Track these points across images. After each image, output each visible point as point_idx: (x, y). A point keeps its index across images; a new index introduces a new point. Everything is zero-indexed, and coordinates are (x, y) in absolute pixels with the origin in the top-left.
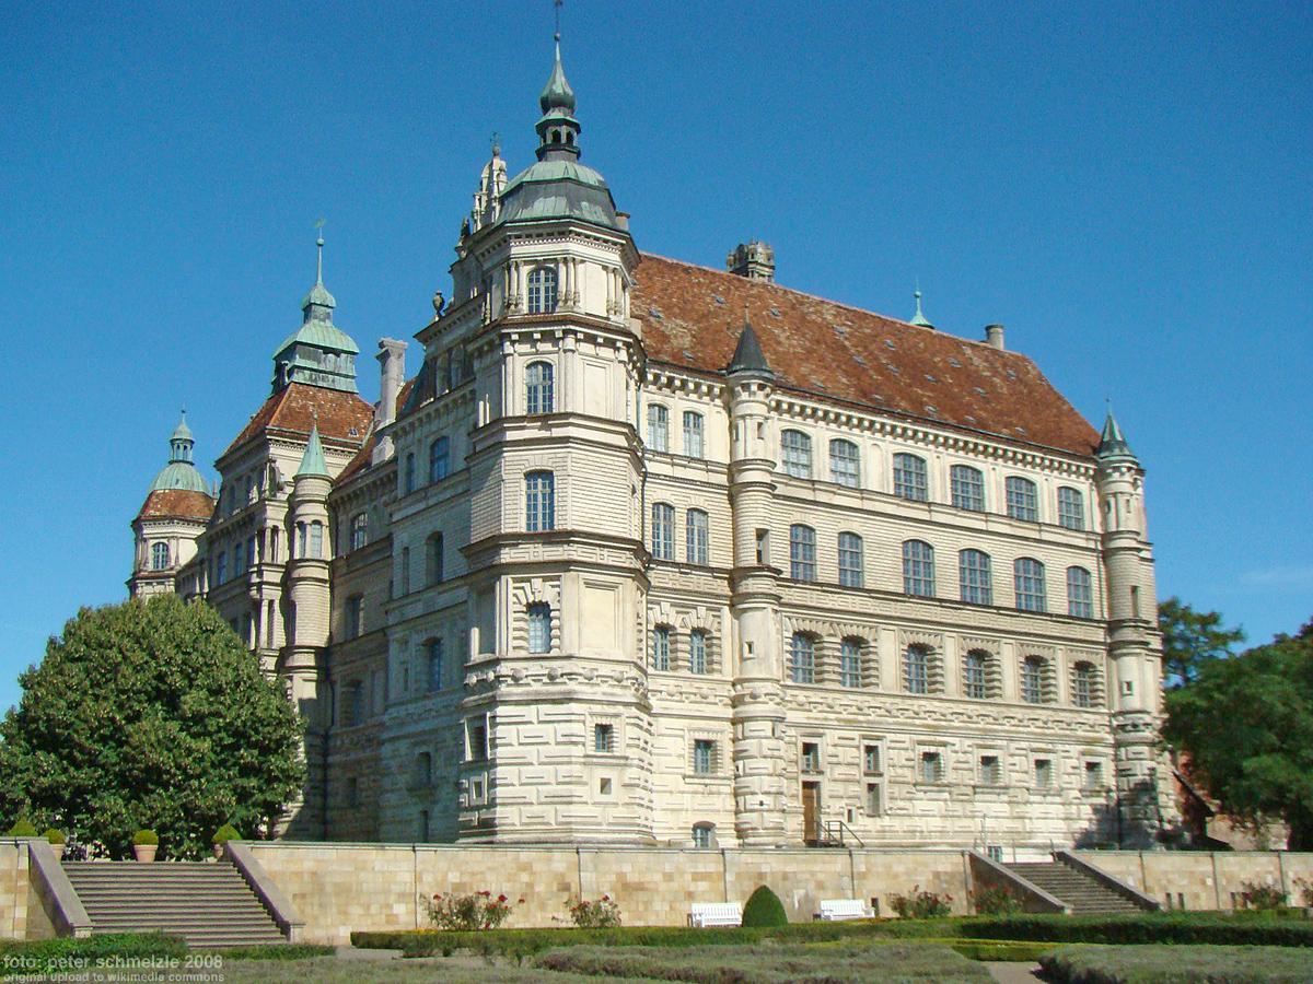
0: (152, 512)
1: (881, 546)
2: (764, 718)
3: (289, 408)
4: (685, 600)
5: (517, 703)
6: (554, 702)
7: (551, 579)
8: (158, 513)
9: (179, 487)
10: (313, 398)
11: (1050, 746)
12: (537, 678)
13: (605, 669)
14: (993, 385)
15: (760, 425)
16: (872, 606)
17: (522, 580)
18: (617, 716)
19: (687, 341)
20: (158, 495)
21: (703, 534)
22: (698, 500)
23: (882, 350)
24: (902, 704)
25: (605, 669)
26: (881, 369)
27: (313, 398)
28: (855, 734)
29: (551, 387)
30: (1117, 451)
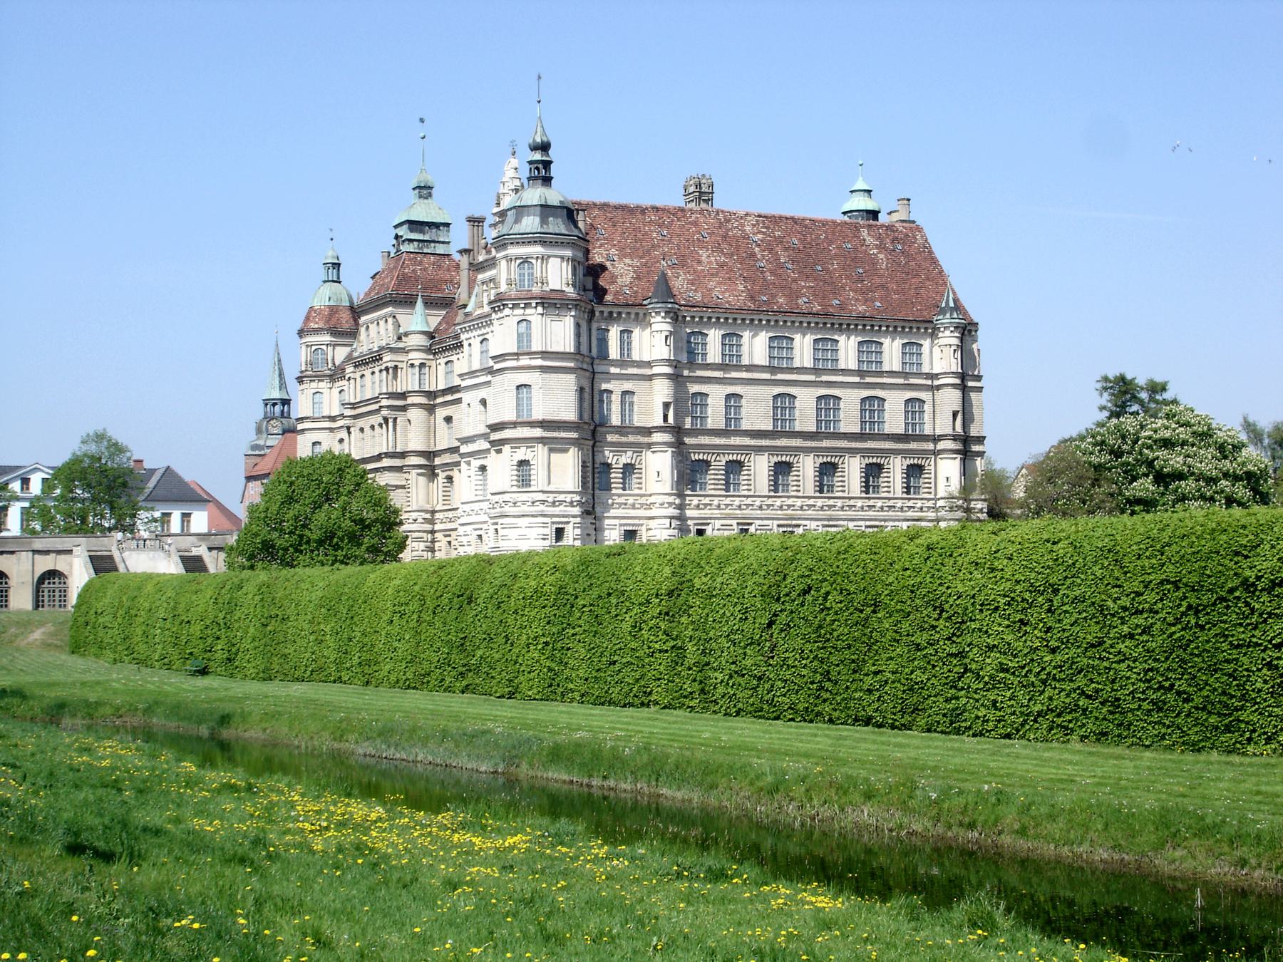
0: (313, 325)
1: (756, 400)
2: (665, 517)
3: (404, 274)
4: (620, 447)
5: (514, 517)
6: (533, 516)
7: (531, 447)
8: (316, 326)
9: (332, 303)
10: (420, 263)
11: (882, 523)
12: (524, 502)
13: (561, 497)
14: (874, 262)
15: (666, 337)
16: (747, 441)
17: (516, 448)
18: (568, 523)
19: (628, 278)
20: (315, 312)
21: (631, 404)
22: (628, 386)
23: (786, 249)
24: (770, 501)
25: (561, 497)
26: (778, 268)
27: (420, 263)
28: (734, 523)
29: (529, 335)
30: (948, 316)
